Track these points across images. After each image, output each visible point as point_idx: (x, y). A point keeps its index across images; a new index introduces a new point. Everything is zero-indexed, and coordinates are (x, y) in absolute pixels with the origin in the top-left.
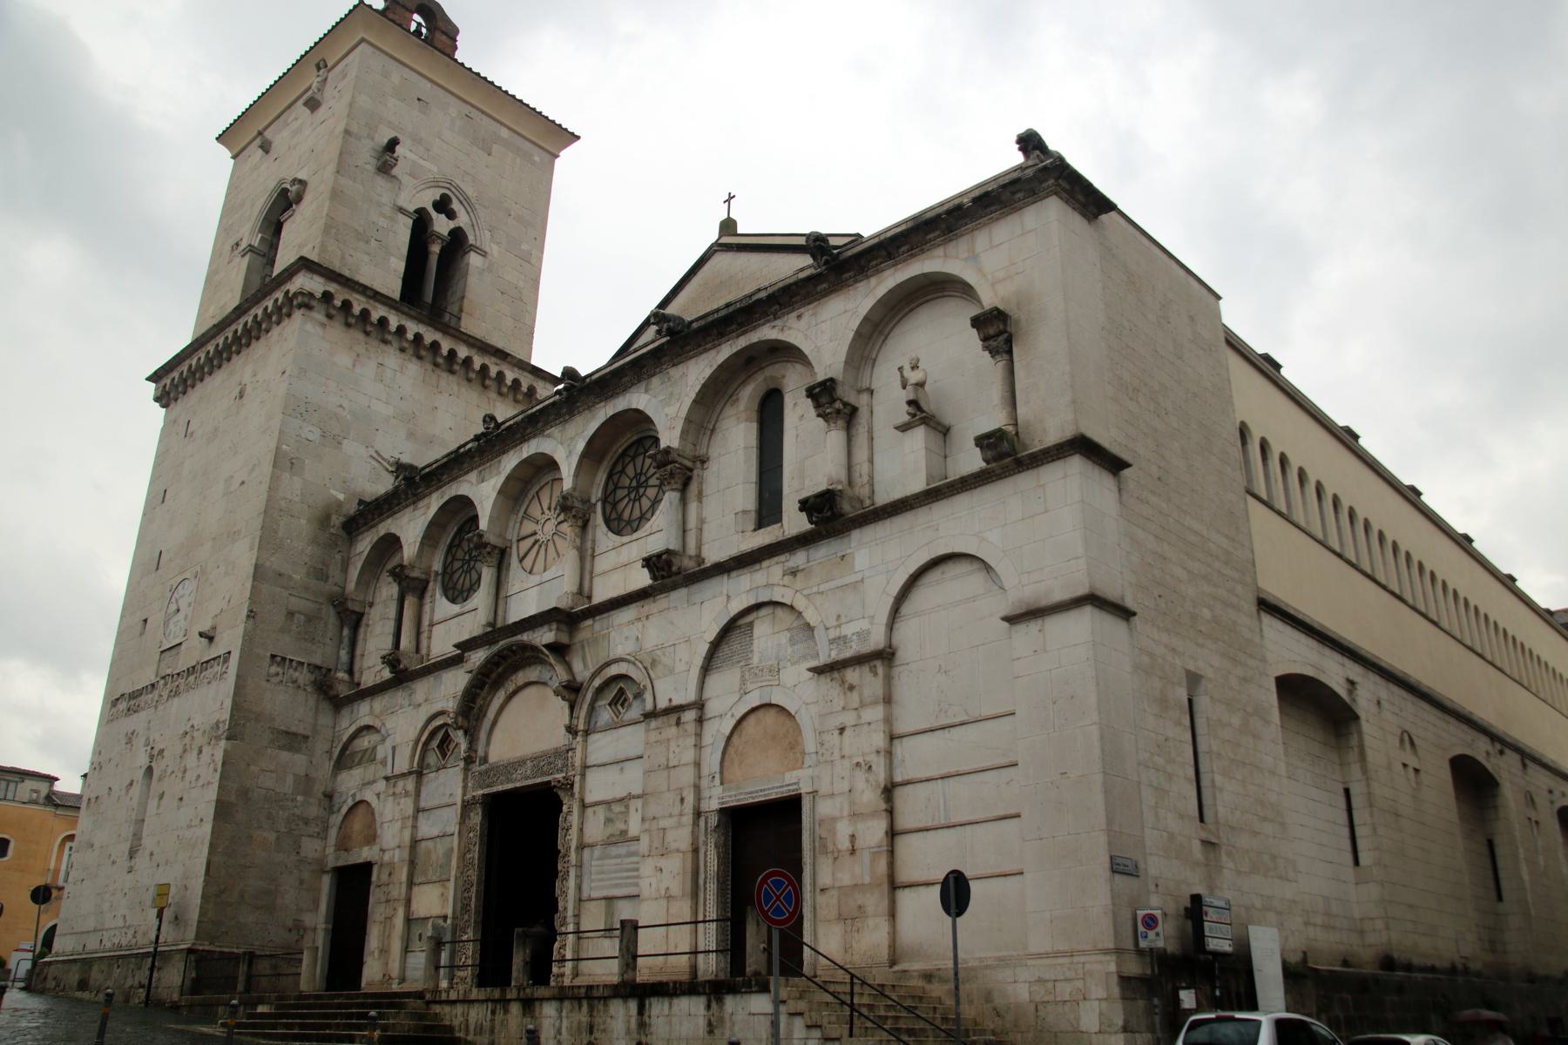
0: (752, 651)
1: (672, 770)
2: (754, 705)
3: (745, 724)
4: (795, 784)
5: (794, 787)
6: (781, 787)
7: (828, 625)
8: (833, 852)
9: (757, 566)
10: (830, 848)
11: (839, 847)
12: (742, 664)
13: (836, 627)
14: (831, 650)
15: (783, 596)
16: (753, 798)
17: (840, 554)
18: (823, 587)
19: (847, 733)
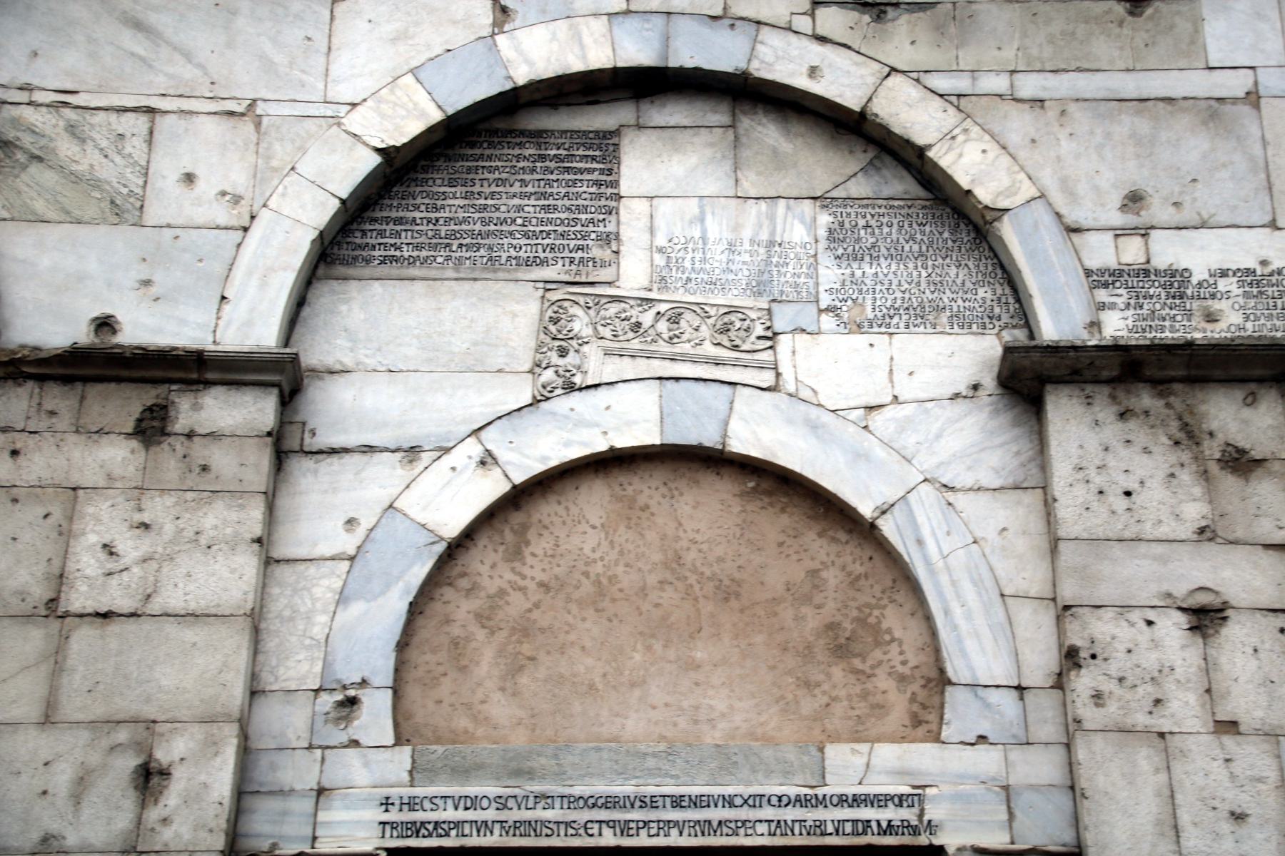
1: (84, 639)
2: (625, 440)
3: (547, 510)
4: (900, 800)
6: (801, 801)
7: (1075, 216)
12: (550, 273)
13: (1120, 233)
14: (1102, 307)
15: (813, 72)
16: (625, 828)
18: (1029, 86)
19: (1237, 632)
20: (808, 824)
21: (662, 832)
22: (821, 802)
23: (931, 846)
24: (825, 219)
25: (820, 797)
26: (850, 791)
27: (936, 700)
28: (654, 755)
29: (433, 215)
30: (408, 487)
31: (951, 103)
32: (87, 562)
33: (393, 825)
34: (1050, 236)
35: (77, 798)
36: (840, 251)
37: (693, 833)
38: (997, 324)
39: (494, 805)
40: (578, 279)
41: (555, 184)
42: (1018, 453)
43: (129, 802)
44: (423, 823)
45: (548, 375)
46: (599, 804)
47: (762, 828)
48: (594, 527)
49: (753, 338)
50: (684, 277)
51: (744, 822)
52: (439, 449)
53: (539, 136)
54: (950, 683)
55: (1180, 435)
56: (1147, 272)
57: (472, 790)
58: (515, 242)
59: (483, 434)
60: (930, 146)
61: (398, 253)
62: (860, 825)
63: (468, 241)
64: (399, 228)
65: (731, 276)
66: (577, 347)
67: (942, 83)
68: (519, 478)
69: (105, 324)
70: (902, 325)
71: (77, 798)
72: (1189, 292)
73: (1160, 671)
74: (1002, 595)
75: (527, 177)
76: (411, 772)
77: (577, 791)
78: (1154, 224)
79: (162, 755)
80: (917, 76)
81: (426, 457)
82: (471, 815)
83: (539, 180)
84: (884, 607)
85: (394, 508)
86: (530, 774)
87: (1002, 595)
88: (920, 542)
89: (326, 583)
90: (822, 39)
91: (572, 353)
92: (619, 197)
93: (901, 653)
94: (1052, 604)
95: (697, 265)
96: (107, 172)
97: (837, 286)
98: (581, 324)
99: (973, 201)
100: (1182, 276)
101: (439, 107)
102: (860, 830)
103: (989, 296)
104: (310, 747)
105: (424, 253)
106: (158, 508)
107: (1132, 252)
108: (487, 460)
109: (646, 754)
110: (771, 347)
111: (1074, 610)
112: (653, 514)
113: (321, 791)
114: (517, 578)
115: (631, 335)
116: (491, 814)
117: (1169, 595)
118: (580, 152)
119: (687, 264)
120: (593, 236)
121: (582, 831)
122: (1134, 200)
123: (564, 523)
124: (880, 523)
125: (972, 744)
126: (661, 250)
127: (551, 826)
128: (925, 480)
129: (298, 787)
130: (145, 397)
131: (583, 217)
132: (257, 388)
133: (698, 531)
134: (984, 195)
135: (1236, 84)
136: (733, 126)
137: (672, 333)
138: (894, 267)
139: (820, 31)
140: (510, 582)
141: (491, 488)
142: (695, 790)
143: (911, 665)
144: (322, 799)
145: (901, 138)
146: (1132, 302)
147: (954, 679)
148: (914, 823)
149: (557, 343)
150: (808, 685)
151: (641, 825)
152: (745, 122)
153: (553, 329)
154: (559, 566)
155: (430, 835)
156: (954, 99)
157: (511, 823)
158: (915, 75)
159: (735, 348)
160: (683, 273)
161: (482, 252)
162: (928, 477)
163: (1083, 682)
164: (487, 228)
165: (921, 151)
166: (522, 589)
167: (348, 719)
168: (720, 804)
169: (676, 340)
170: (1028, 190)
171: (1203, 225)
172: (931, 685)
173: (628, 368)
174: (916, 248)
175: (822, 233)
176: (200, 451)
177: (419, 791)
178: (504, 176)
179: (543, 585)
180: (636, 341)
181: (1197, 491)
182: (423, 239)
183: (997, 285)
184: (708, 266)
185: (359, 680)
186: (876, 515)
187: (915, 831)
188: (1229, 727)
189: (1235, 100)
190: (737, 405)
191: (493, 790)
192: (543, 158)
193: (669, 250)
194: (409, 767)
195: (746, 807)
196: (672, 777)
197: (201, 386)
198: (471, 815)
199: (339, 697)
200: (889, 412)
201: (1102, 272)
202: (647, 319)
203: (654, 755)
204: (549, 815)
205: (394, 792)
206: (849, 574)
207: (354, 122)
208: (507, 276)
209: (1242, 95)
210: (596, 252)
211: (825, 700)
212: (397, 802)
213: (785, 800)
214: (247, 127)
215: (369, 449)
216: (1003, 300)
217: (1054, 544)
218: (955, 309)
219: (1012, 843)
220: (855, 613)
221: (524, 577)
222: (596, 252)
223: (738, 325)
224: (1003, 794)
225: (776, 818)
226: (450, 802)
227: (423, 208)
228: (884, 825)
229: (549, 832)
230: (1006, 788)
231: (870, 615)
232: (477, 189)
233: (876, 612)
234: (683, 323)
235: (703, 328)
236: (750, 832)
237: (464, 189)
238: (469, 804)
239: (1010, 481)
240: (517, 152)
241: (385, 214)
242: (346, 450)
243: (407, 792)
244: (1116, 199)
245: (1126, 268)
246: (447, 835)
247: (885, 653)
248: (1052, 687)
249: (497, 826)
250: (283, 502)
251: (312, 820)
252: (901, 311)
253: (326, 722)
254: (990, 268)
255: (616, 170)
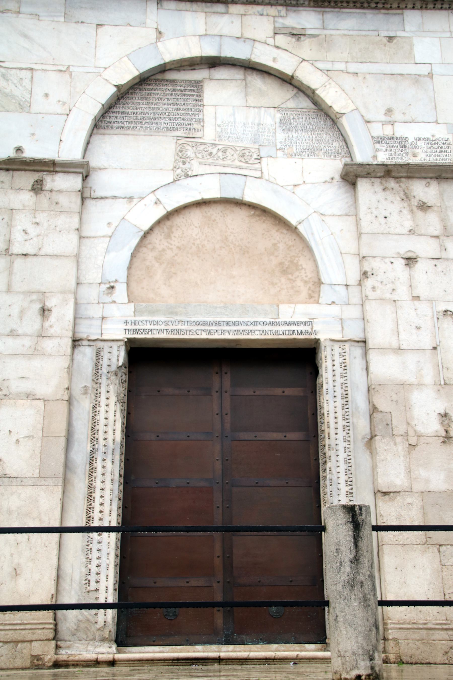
0: (200, 121)
1: (19, 262)
2: (207, 196)
3: (178, 220)
4: (305, 323)
5: (302, 328)
6: (271, 324)
7: (368, 117)
8: (406, 435)
9: (220, 8)
10: (400, 429)
11: (420, 429)
12: (179, 133)
13: (384, 123)
14: (377, 150)
15: (274, 60)
16: (210, 332)
17: (386, 34)
18: (353, 67)
19: (420, 266)
20: (273, 331)
21: (222, 334)
22: (278, 324)
23: (315, 339)
24: (278, 116)
25: (278, 322)
26: (288, 320)
27: (317, 289)
28: (220, 308)
29: (135, 111)
30: (129, 211)
31: (324, 73)
32: (18, 236)
33: (129, 330)
34: (360, 123)
35: (21, 318)
36: (284, 128)
37: (233, 334)
38: (340, 156)
39: (164, 324)
40: (189, 136)
41: (180, 100)
42: (347, 203)
43: (38, 319)
44: (139, 330)
45: (179, 171)
46: (201, 324)
47: (258, 333)
48: (196, 227)
49: (253, 159)
50: (228, 136)
51: (251, 331)
52: (140, 198)
53: (173, 82)
54: (322, 283)
55: (404, 197)
56: (393, 138)
57: (156, 318)
58: (166, 122)
59: (156, 193)
60: (317, 89)
61: (123, 125)
62: (291, 332)
63: (148, 121)
64: (123, 115)
65: (245, 136)
66: (189, 161)
67: (321, 65)
68: (170, 209)
69: (19, 149)
70: (306, 155)
71: (21, 318)
72: (408, 146)
73: (395, 279)
74: (341, 253)
75: (169, 97)
76: (134, 312)
77: (193, 319)
78: (396, 120)
79: (48, 304)
80: (312, 62)
81: (135, 201)
82: (156, 327)
83: (174, 98)
84: (300, 257)
85: (125, 219)
86: (176, 314)
87: (341, 253)
88: (312, 234)
89: (102, 245)
90: (278, 47)
91: (187, 163)
92: (203, 106)
93: (305, 273)
94: (358, 256)
95: (232, 132)
96: (17, 92)
97: (283, 140)
98: (190, 152)
99: (332, 110)
100: (405, 140)
101: (137, 70)
102: (291, 333)
103: (337, 145)
104: (99, 303)
105: (132, 125)
106: (41, 217)
107: (388, 131)
108: (157, 202)
109: (216, 307)
110: (259, 163)
111: (366, 258)
112: (217, 223)
113: (103, 318)
114: (169, 245)
115: (209, 157)
116: (163, 327)
117: (399, 253)
118: (189, 88)
119: (229, 131)
120: (194, 120)
121: (195, 333)
122: (389, 111)
123: (185, 225)
124: (299, 227)
125: (330, 304)
126: (219, 126)
127: (184, 331)
128: (315, 212)
129: (95, 316)
130: (36, 176)
131: (190, 113)
132: (74, 174)
133: (233, 229)
134: (337, 108)
135: (424, 70)
136: (245, 80)
137: (223, 157)
138: (303, 134)
139: (277, 44)
140: (166, 246)
141: (160, 212)
142: (234, 320)
143: (309, 277)
144: (104, 321)
145: (306, 86)
146: (388, 149)
147: (324, 282)
148: (310, 331)
149: (182, 160)
150: (273, 284)
151: (215, 331)
152: (249, 78)
153: (180, 154)
154: (184, 241)
155: (142, 334)
156: (325, 72)
157: (170, 330)
158: (311, 62)
159: (247, 162)
160: (227, 134)
161: (154, 125)
162: (316, 210)
163: (369, 283)
164: (155, 116)
165: (313, 91)
166: (171, 249)
167: (111, 293)
168: (243, 324)
169: (225, 159)
170: (352, 107)
171: (413, 121)
172: (316, 284)
173: (208, 169)
174: (311, 127)
175: (278, 121)
176: (55, 196)
177: (138, 319)
178: (161, 97)
179: (179, 248)
180: (211, 159)
181: (409, 217)
182: (132, 120)
183: (340, 142)
184: (236, 132)
185: (115, 280)
186: (297, 224)
187: (310, 334)
188: (417, 298)
189: (424, 76)
190: (247, 183)
191: (163, 319)
192: (175, 90)
193: (222, 126)
194: (133, 310)
195: (252, 325)
196: (226, 315)
197: (54, 173)
198: (156, 327)
199: (108, 286)
200: (303, 187)
201: (378, 138)
202: (214, 151)
203: (220, 308)
204: (183, 327)
205: (129, 319)
206: (287, 245)
207: (106, 74)
208: (163, 134)
209: (427, 74)
210: (195, 126)
211: (279, 289)
212: (130, 322)
213: (265, 323)
214: (67, 76)
215: (115, 197)
216: (342, 147)
217: (360, 235)
218: (325, 150)
219: (343, 337)
220: (289, 259)
221: (171, 245)
222: (195, 126)
223: (247, 154)
224: (340, 322)
225: (262, 329)
226: (148, 323)
227: (131, 108)
228: (299, 332)
229: (183, 333)
230: (341, 319)
231: (295, 259)
232: (151, 101)
233: (297, 259)
234: (227, 153)
235: (235, 155)
236: (253, 334)
237: (146, 101)
238: (155, 323)
239: (344, 213)
240: (165, 87)
241: (118, 110)
242: (106, 198)
243: (133, 319)
244: (383, 111)
245: (386, 136)
246: (148, 333)
247: (300, 273)
248: (357, 285)
249: (165, 331)
250: (84, 216)
251: (100, 328)
252: (306, 150)
253: (104, 294)
254: (338, 135)
255: (202, 95)
